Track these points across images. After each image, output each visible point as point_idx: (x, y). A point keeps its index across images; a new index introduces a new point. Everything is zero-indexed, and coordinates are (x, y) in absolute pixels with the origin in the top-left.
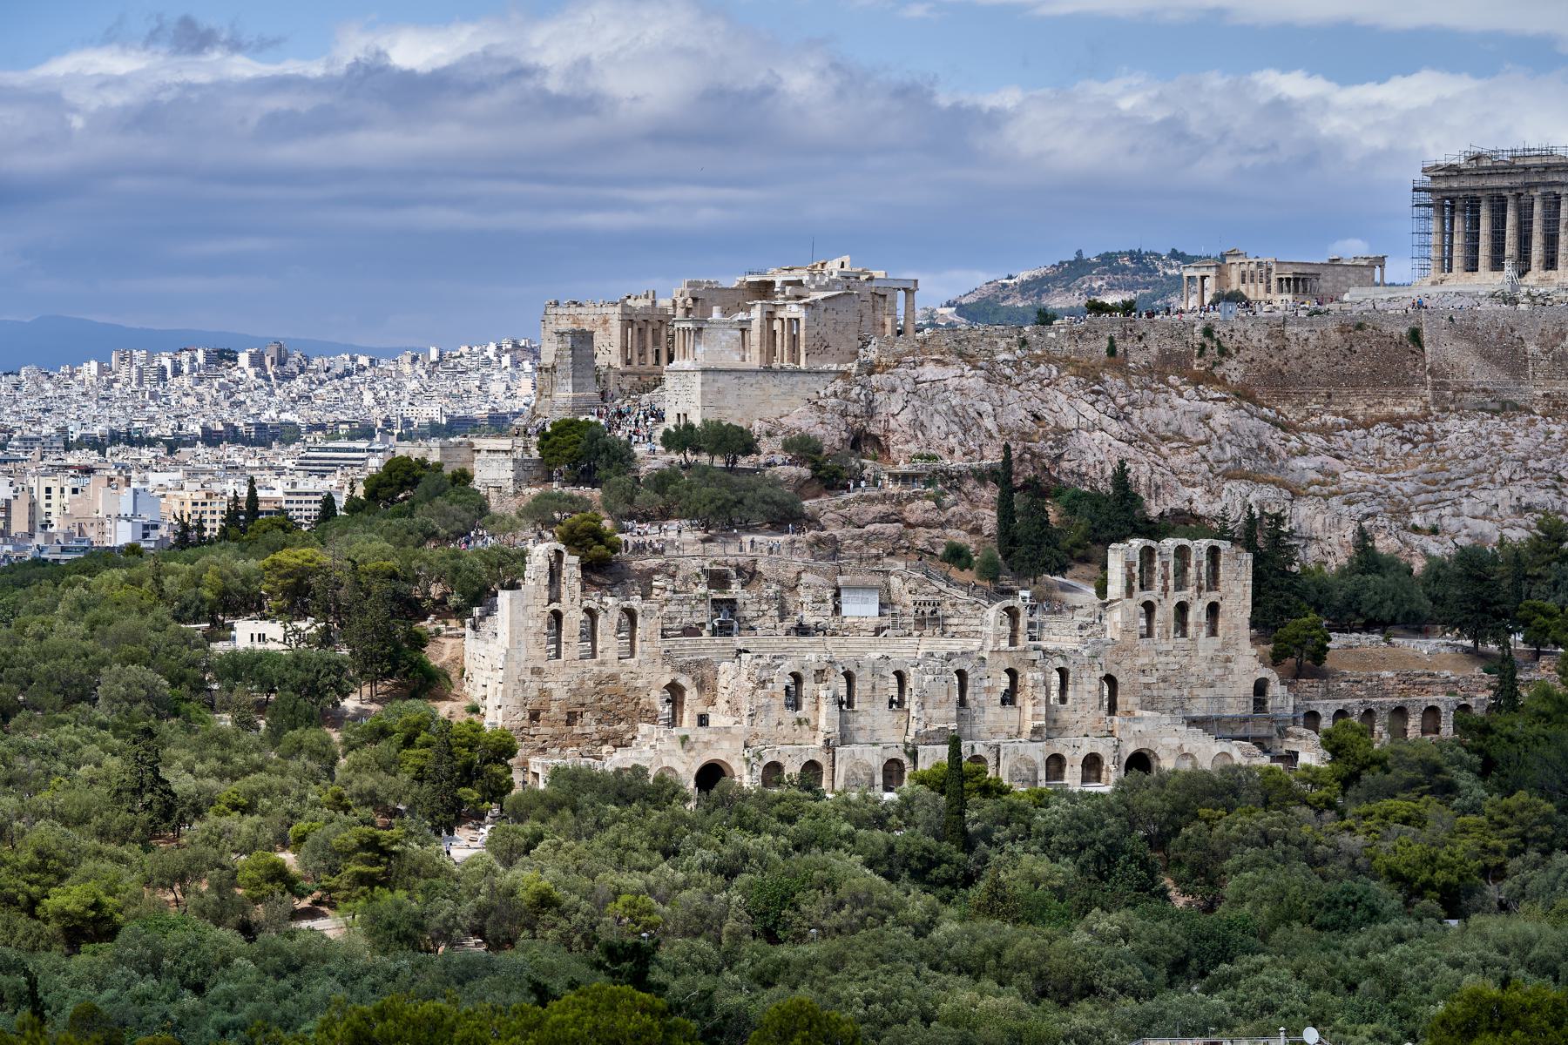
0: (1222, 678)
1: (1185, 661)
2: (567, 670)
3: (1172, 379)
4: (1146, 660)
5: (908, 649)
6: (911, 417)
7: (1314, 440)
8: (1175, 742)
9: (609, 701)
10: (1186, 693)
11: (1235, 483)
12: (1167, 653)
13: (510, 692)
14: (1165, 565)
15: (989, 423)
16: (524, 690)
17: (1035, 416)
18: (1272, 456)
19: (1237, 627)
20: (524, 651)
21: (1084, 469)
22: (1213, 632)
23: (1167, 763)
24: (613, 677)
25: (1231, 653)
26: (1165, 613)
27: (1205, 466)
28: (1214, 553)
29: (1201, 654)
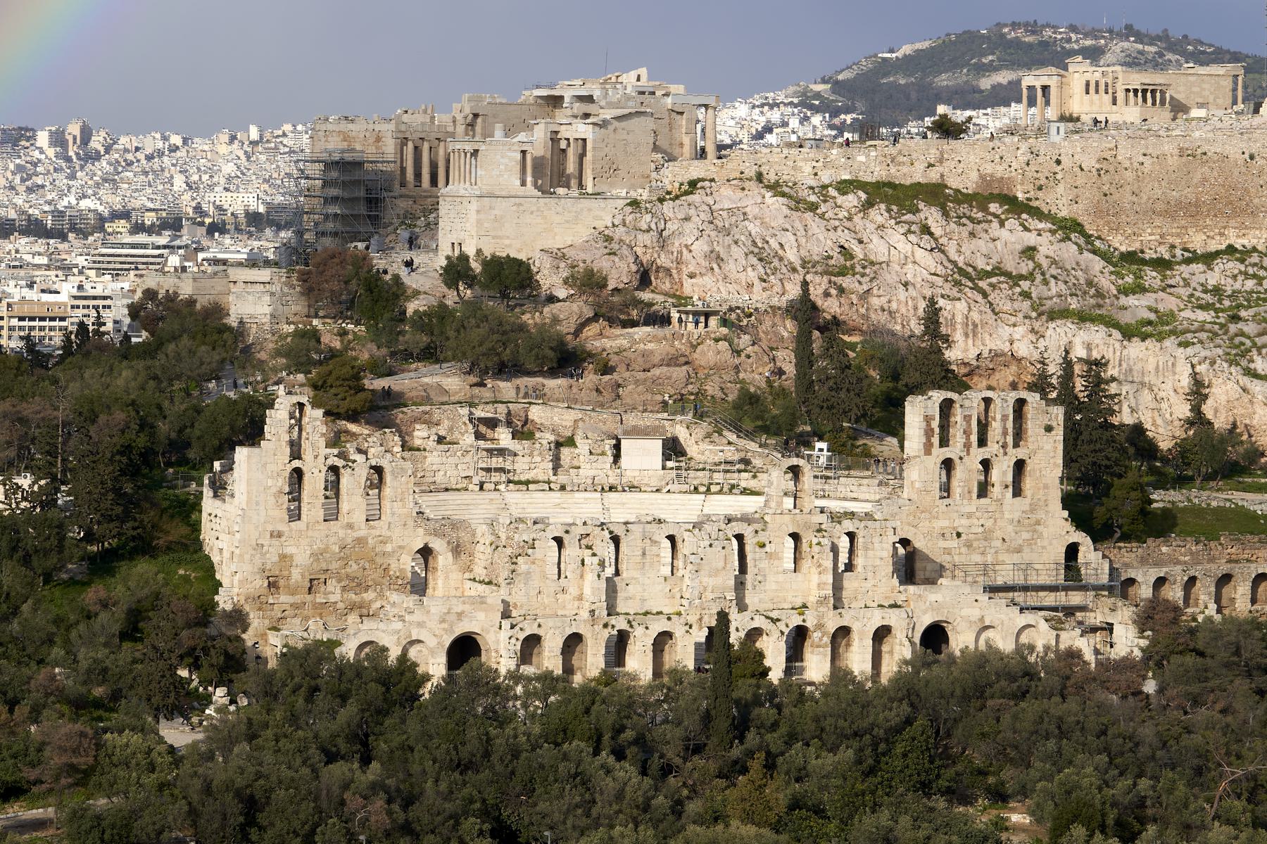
0: (1030, 542)
1: (989, 524)
2: (310, 533)
3: (993, 207)
4: (946, 523)
5: (681, 508)
6: (706, 248)
7: (1151, 277)
8: (975, 613)
9: (355, 567)
10: (989, 559)
11: (1059, 322)
12: (970, 515)
13: (247, 557)
14: (967, 418)
15: (792, 255)
16: (263, 555)
17: (842, 247)
18: (1100, 294)
19: (1046, 487)
20: (263, 513)
21: (894, 306)
22: (1017, 492)
23: (961, 640)
24: (360, 541)
25: (1040, 515)
26: (968, 472)
27: (1027, 304)
28: (1021, 403)
29: (1007, 516)
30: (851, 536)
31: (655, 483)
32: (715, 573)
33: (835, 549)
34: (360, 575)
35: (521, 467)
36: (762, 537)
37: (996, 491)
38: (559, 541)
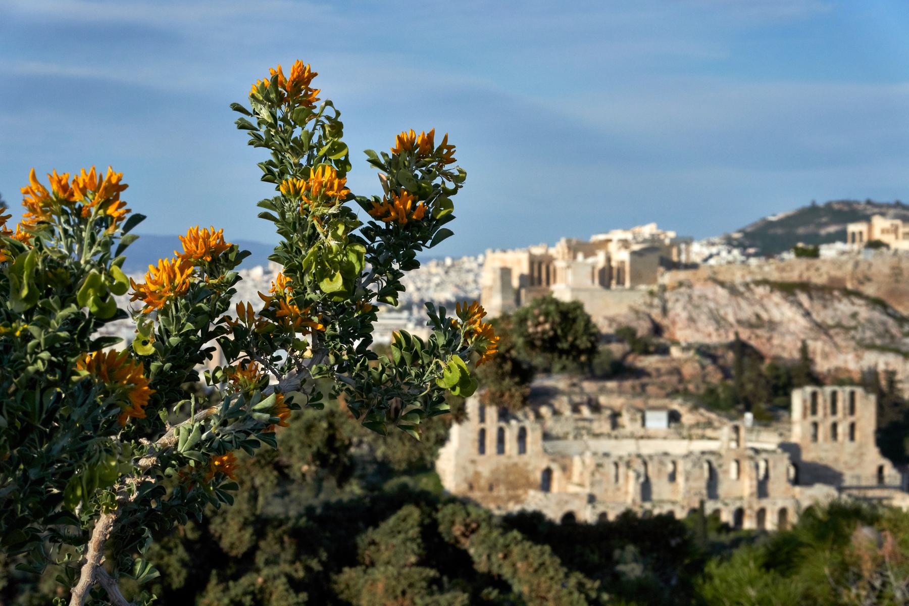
0: (859, 464)
5: (678, 447)
12: (826, 451)
18: (893, 337)
24: (515, 465)
28: (852, 394)
30: (766, 461)
31: (663, 434)
32: (696, 480)
33: (757, 467)
34: (516, 481)
35: (596, 427)
36: (721, 462)
37: (840, 437)
38: (616, 465)
